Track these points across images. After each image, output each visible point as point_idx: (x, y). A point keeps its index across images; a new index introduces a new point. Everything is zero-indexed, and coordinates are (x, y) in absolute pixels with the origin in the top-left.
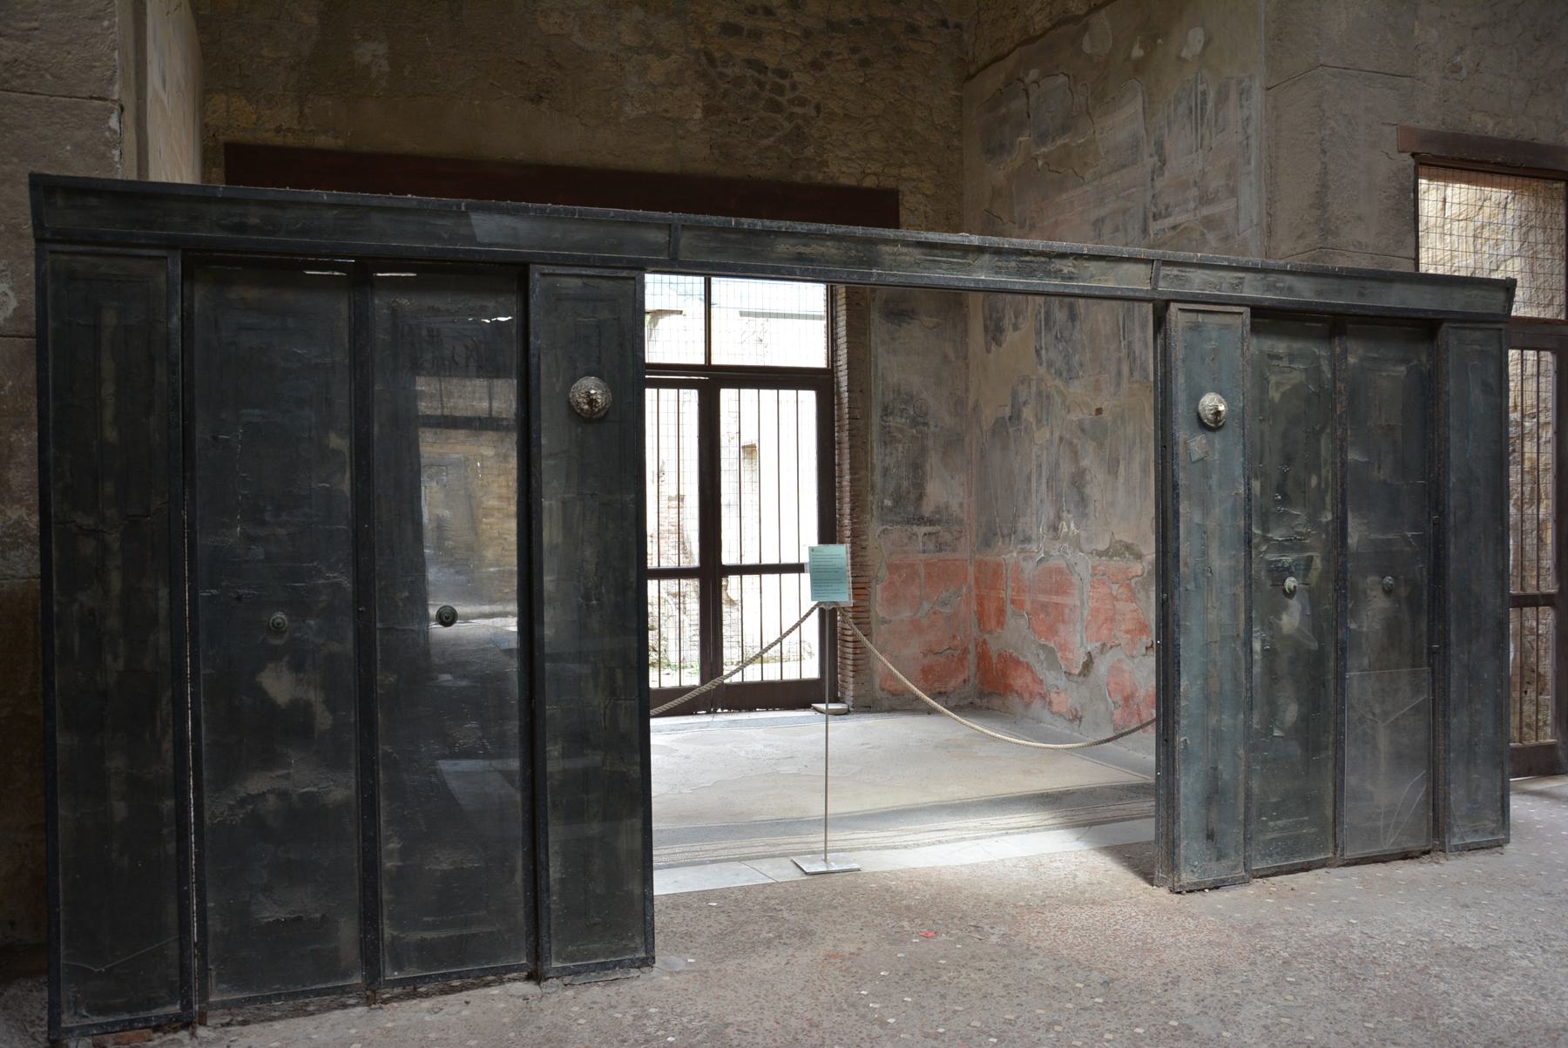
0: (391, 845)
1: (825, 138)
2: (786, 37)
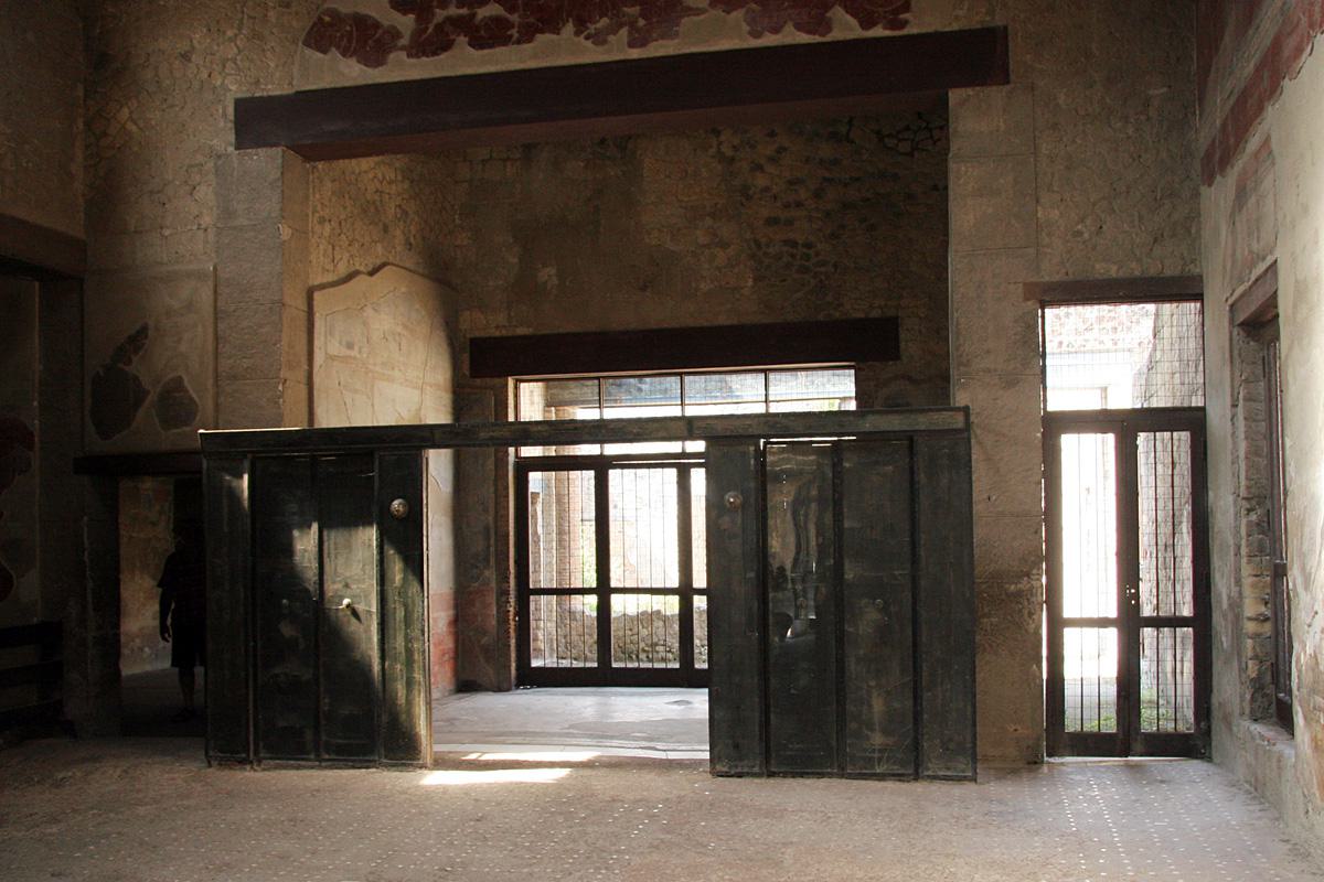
1: (840, 286)
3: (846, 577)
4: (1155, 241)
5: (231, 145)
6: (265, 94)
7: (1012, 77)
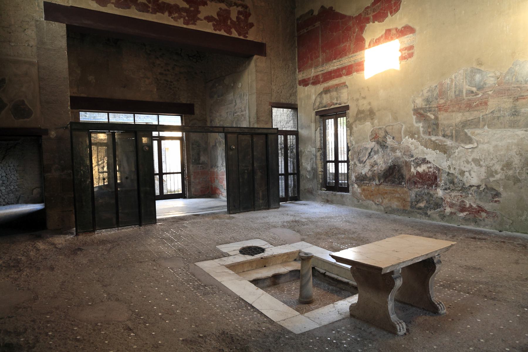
7: (267, 55)
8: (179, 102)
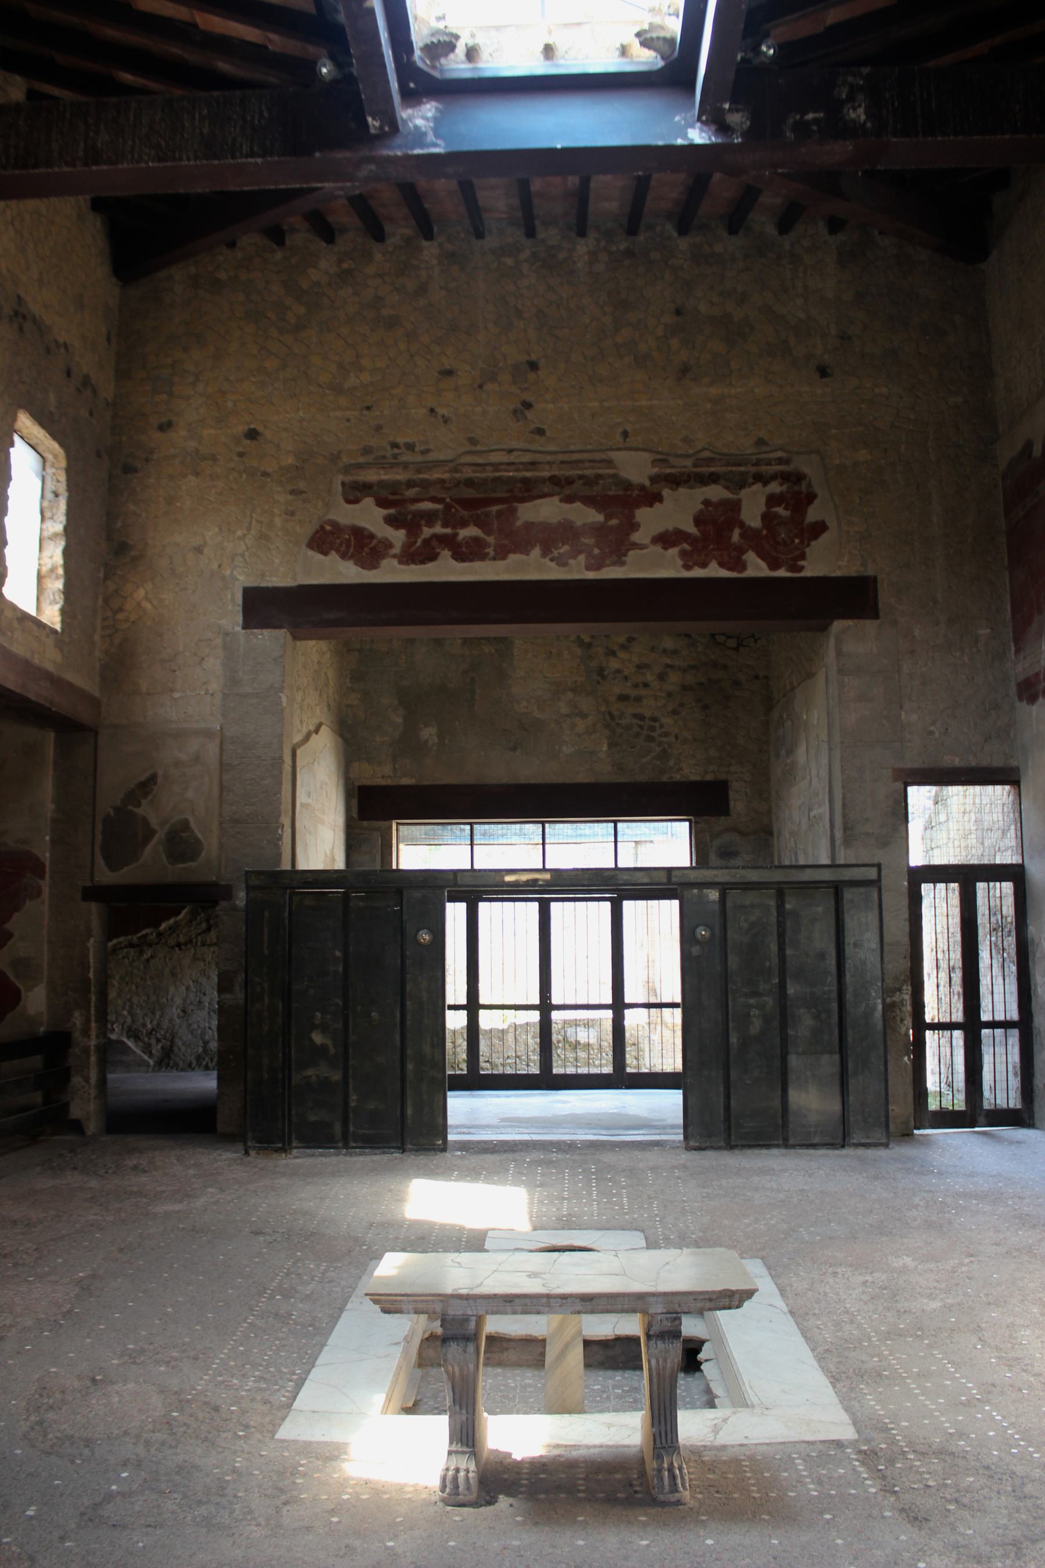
0: (353, 1097)
2: (656, 698)
3: (788, 992)
4: (986, 740)
5: (238, 625)
6: (270, 585)
7: (881, 614)
8: (678, 777)
